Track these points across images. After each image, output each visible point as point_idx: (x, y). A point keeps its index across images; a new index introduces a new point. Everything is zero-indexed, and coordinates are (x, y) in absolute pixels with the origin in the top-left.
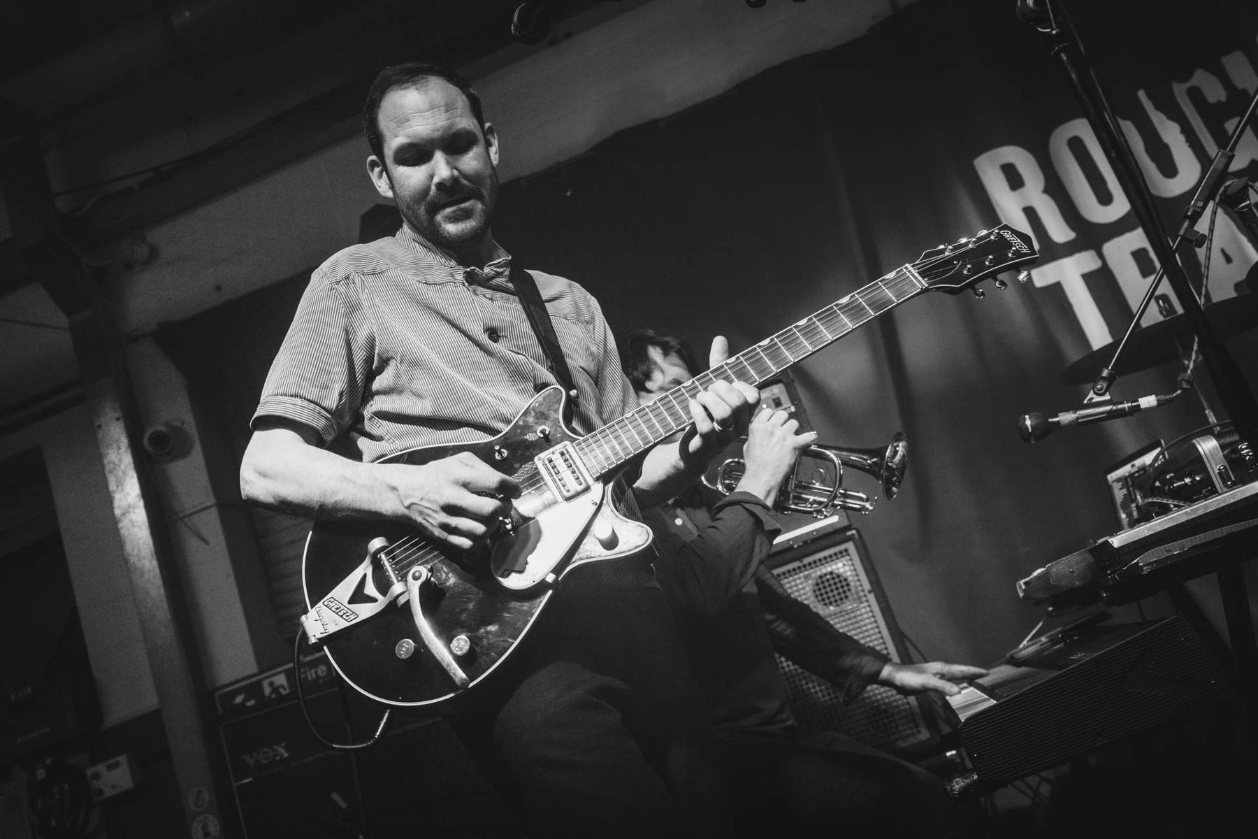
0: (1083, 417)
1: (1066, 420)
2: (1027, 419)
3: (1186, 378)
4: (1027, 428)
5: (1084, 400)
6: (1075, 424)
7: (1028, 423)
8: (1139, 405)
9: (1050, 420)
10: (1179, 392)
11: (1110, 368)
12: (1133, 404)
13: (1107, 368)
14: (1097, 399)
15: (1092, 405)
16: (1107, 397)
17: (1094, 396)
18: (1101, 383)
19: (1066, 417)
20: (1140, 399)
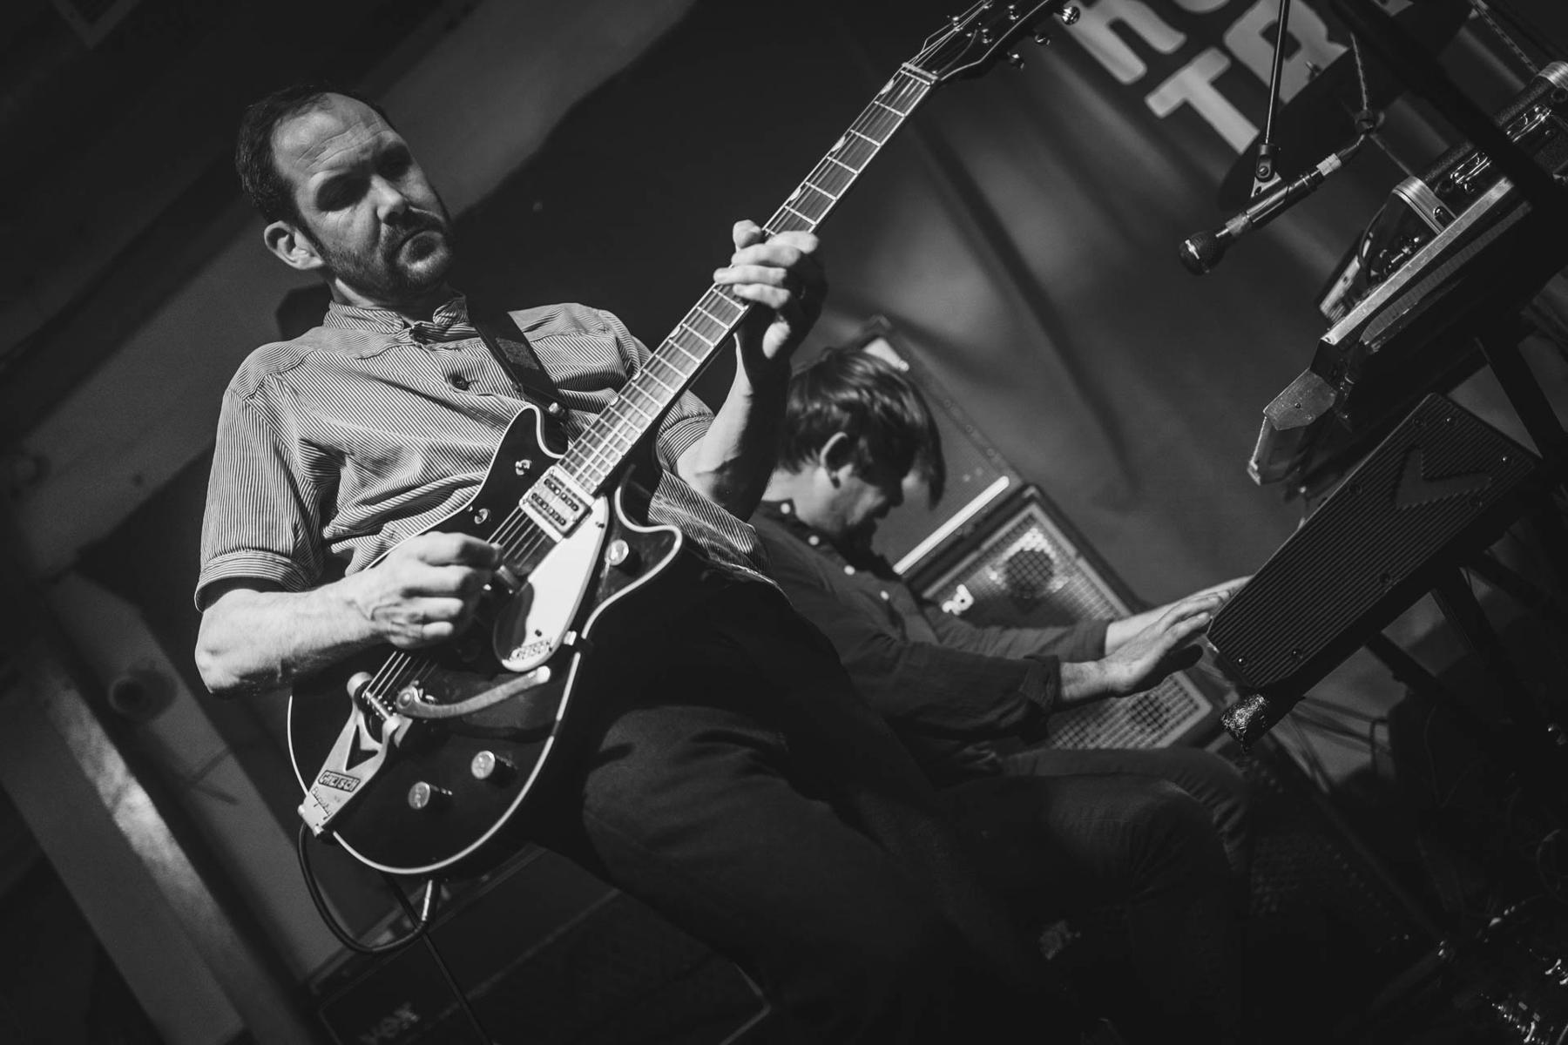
0: (1256, 215)
1: (1236, 227)
2: (1189, 244)
3: (1365, 117)
4: (1193, 255)
5: (1250, 194)
6: (1251, 227)
7: (1192, 249)
8: (1320, 173)
9: (1218, 235)
10: (1362, 138)
11: (1267, 141)
12: (1312, 175)
13: (1264, 143)
14: (1265, 186)
15: (1263, 196)
16: (1277, 179)
17: (1261, 184)
18: (1262, 165)
19: (1237, 224)
20: (1318, 166)
